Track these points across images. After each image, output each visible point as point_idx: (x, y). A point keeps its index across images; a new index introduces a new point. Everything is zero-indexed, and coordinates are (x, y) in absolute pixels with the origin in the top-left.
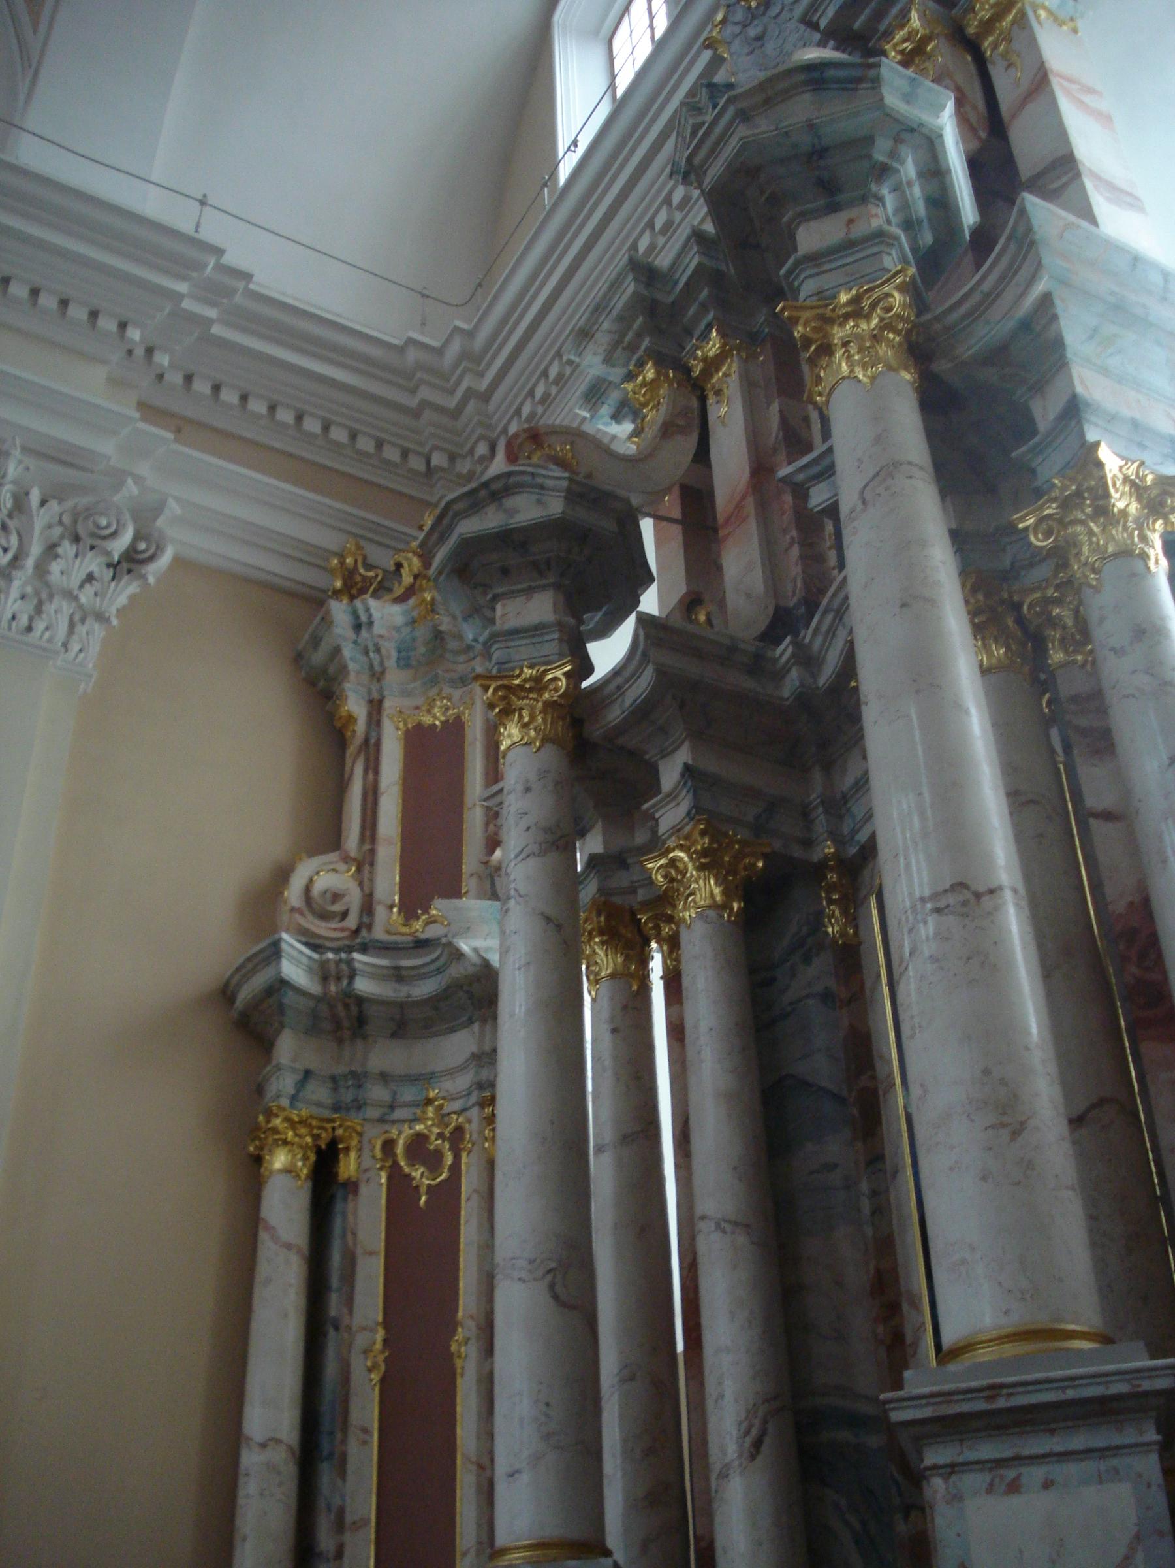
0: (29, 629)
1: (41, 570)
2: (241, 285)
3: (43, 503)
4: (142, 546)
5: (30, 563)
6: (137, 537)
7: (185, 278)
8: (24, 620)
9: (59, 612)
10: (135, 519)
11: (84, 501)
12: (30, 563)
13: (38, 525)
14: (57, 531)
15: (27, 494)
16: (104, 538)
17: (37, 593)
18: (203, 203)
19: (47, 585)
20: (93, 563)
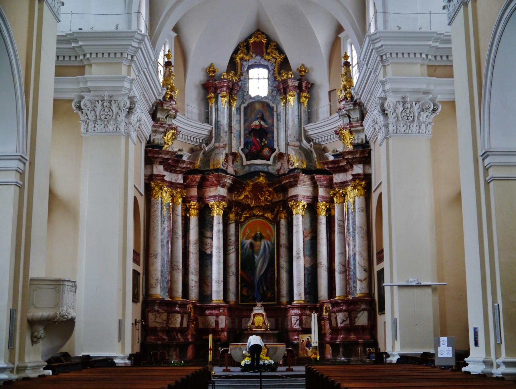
0: (419, 132)
1: (418, 118)
2: (442, 36)
3: (416, 104)
4: (435, 107)
5: (416, 118)
6: (434, 106)
7: (430, 40)
8: (418, 131)
9: (423, 126)
10: (432, 101)
11: (422, 102)
12: (416, 118)
13: (416, 109)
14: (419, 110)
15: (412, 103)
16: (428, 109)
17: (419, 124)
18: (430, 14)
19: (420, 122)
20: (427, 113)
